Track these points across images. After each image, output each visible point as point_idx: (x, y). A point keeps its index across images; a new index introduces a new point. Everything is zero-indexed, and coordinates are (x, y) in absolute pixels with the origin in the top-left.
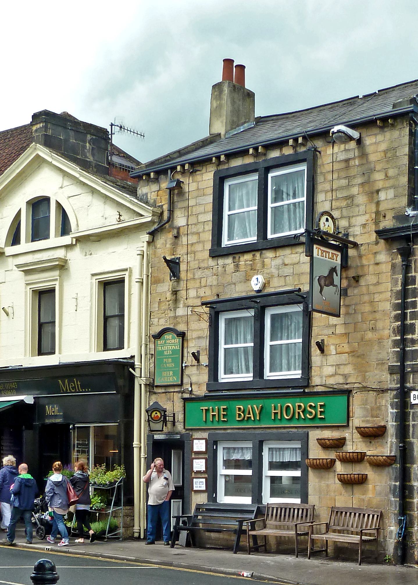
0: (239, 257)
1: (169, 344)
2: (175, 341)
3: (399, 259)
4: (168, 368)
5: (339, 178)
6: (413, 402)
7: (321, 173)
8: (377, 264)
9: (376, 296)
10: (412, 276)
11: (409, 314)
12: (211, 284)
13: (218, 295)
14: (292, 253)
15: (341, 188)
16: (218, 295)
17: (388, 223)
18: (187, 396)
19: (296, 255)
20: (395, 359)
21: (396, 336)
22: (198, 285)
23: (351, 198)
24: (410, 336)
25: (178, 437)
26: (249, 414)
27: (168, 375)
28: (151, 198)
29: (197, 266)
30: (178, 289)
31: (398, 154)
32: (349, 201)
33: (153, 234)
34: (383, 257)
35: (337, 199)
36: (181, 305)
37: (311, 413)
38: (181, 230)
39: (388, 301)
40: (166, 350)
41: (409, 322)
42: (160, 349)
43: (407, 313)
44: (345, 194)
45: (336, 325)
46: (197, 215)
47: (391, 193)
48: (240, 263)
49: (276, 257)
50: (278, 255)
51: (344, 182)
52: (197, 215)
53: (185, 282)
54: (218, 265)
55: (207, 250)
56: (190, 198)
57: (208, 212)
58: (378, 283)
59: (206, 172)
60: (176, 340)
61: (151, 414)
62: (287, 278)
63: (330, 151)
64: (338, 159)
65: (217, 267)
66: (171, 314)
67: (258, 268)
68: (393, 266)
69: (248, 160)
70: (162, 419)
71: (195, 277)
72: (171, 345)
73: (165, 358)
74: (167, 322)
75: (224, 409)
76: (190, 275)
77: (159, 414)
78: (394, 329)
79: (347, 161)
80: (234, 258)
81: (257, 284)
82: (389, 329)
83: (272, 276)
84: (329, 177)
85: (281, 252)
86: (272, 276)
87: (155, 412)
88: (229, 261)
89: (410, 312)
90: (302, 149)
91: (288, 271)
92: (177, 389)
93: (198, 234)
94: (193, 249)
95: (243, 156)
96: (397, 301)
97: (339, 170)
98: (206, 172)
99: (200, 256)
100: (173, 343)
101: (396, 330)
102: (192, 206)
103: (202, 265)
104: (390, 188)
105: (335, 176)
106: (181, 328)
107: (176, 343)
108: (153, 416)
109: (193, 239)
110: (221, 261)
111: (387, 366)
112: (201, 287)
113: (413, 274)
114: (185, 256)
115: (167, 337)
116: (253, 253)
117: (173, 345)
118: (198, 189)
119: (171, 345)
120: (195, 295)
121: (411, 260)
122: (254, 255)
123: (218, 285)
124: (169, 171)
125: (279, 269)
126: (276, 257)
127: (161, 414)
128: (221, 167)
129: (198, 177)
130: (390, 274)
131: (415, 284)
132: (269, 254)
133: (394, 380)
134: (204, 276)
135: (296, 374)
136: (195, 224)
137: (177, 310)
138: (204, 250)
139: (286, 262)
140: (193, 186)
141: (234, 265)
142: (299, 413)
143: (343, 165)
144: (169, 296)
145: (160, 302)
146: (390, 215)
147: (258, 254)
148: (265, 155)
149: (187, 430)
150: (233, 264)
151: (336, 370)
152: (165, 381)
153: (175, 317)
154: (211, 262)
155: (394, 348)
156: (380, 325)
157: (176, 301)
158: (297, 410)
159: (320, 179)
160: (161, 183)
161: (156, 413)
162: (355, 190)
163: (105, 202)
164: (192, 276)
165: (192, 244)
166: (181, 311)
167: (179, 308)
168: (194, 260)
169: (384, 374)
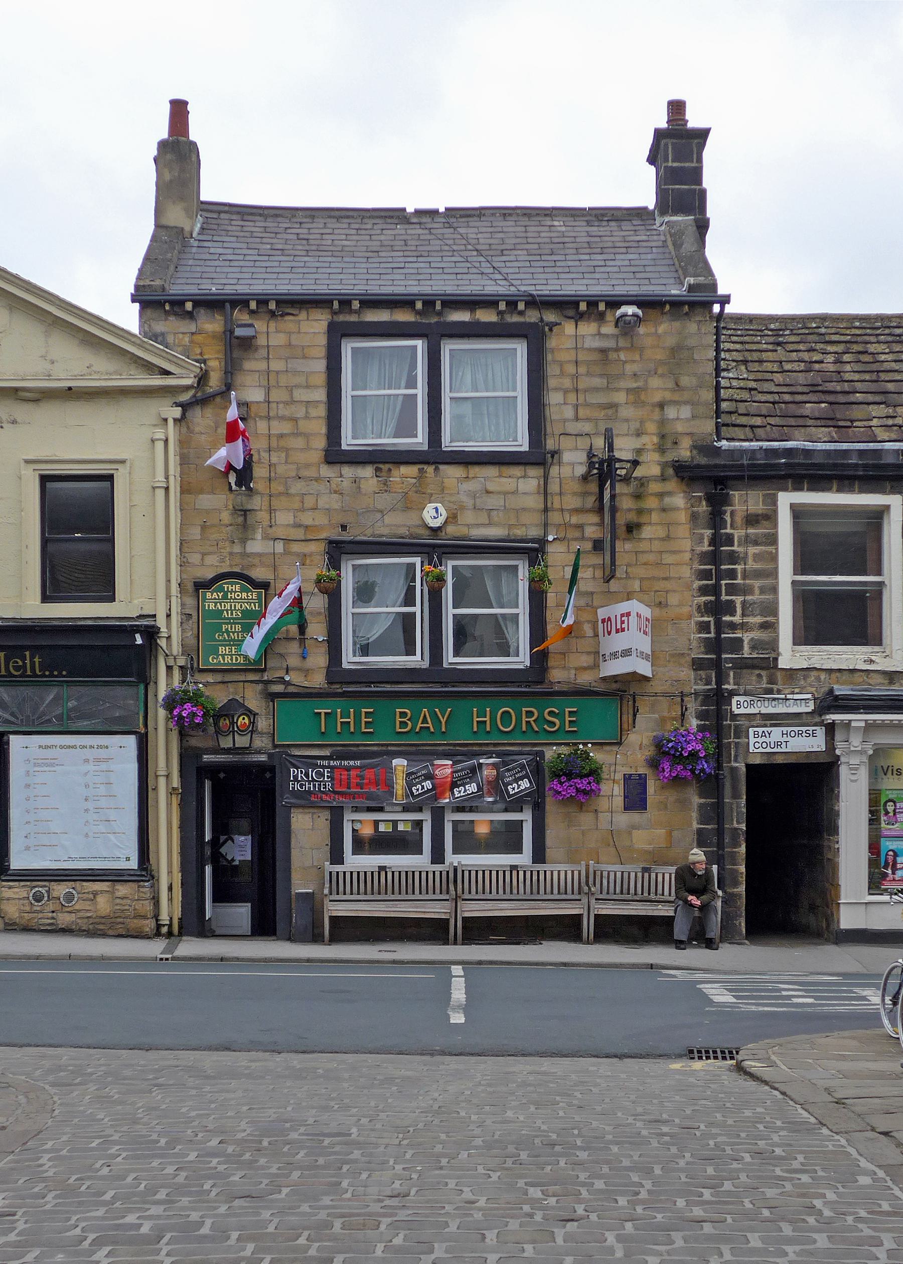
0: (390, 470)
1: (235, 599)
2: (248, 596)
3: (703, 508)
4: (234, 640)
5: (589, 374)
6: (737, 711)
7: (554, 361)
8: (664, 510)
9: (664, 556)
10: (727, 534)
11: (724, 588)
12: (327, 506)
13: (344, 527)
14: (500, 476)
15: (596, 390)
16: (344, 527)
17: (684, 452)
18: (278, 688)
19: (510, 480)
20: (703, 649)
21: (702, 616)
22: (297, 505)
23: (614, 406)
24: (727, 618)
25: (263, 758)
26: (425, 720)
27: (233, 653)
28: (174, 344)
29: (293, 474)
30: (249, 507)
31: (696, 357)
32: (610, 412)
33: (185, 407)
34: (679, 501)
35: (587, 405)
36: (259, 536)
37: (553, 724)
38: (253, 408)
39: (687, 564)
40: (227, 610)
41: (724, 597)
42: (212, 606)
43: (721, 585)
44: (601, 398)
45: (592, 593)
46: (290, 389)
47: (686, 412)
48: (391, 479)
49: (467, 477)
50: (473, 476)
51: (597, 382)
52: (290, 389)
53: (266, 498)
54: (341, 476)
55: (317, 449)
56: (271, 356)
57: (316, 387)
58: (668, 538)
59: (308, 319)
60: (252, 595)
61: (237, 720)
62: (494, 513)
63: (569, 328)
64: (586, 345)
65: (340, 479)
66: (237, 549)
67: (432, 492)
68: (694, 517)
69: (403, 316)
70: (250, 729)
71: (289, 492)
72: (239, 602)
73: (227, 624)
74: (224, 562)
75: (570, 712)
76: (277, 487)
77: (247, 721)
78: (699, 607)
79: (603, 351)
80: (378, 470)
81: (435, 518)
82: (690, 606)
83: (462, 508)
84: (571, 369)
85: (475, 470)
86: (462, 508)
87: (241, 718)
88: (367, 472)
89: (726, 584)
90: (516, 319)
91: (494, 502)
92: (252, 677)
93: (295, 420)
94: (282, 443)
95: (391, 308)
96: (702, 567)
97: (588, 363)
98: (308, 319)
99: (301, 457)
100: (245, 599)
101: (702, 607)
102: (277, 372)
103: (304, 473)
104: (686, 403)
105: (582, 370)
106: (259, 574)
107: (252, 599)
108: (239, 723)
109: (278, 427)
110: (348, 471)
111: (689, 659)
112: (303, 510)
113: (728, 531)
114: (265, 455)
115: (228, 587)
116: (421, 466)
117: (244, 603)
118: (290, 345)
119: (239, 602)
120: (292, 522)
121: (726, 512)
122: (421, 471)
123: (343, 510)
124: (228, 305)
125: (474, 497)
126: (467, 477)
127: (250, 719)
128: (341, 318)
129: (289, 323)
130: (688, 526)
131: (733, 545)
132: (453, 472)
133: (701, 680)
134: (311, 492)
135: (522, 659)
136: (286, 403)
137: (249, 542)
138: (308, 448)
139: (490, 488)
140: (278, 340)
141: (378, 481)
142: (528, 722)
143: (596, 356)
144: (226, 517)
145: (204, 527)
146: (686, 443)
147: (430, 469)
148: (440, 314)
149: (275, 746)
150: (375, 479)
151: (594, 661)
152: (226, 662)
153: (245, 555)
154: (326, 471)
155: (700, 633)
156: (673, 599)
157: (245, 526)
158: (524, 719)
159: (552, 370)
160: (199, 322)
161: (244, 719)
162: (620, 397)
163: (46, 331)
164: (281, 489)
165: (281, 436)
166: (256, 546)
167: (252, 539)
168: (286, 462)
169: (685, 669)
